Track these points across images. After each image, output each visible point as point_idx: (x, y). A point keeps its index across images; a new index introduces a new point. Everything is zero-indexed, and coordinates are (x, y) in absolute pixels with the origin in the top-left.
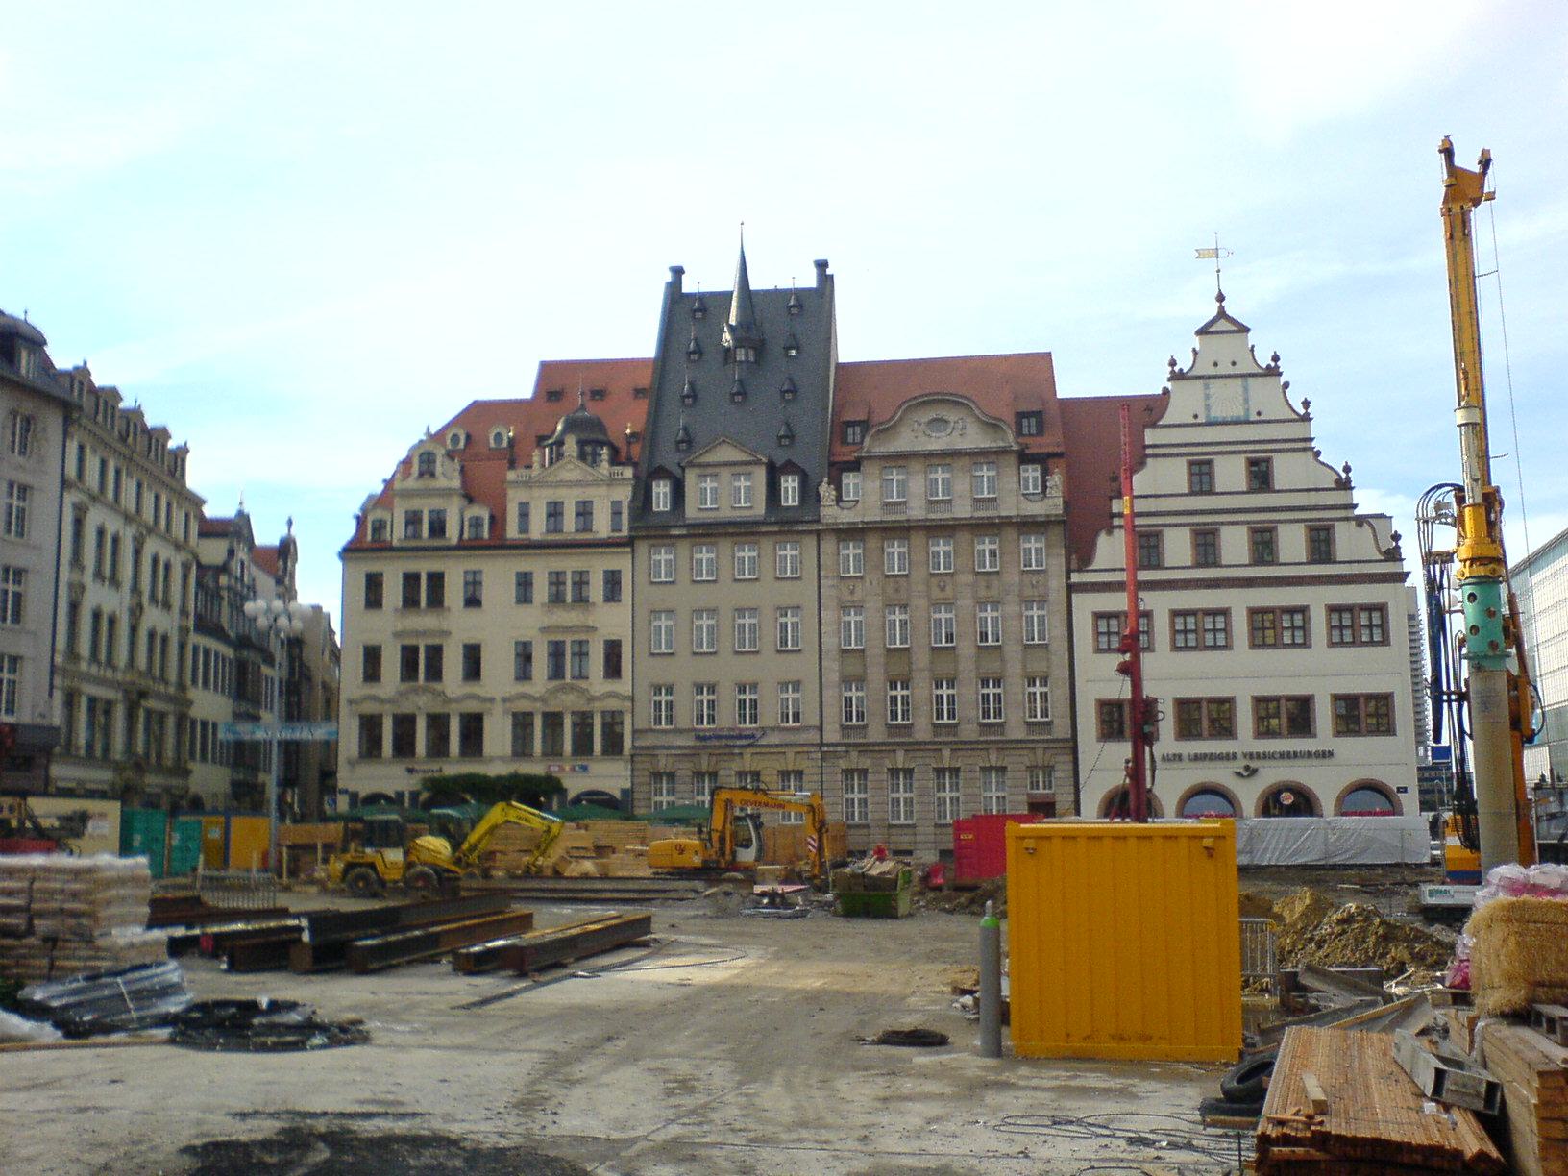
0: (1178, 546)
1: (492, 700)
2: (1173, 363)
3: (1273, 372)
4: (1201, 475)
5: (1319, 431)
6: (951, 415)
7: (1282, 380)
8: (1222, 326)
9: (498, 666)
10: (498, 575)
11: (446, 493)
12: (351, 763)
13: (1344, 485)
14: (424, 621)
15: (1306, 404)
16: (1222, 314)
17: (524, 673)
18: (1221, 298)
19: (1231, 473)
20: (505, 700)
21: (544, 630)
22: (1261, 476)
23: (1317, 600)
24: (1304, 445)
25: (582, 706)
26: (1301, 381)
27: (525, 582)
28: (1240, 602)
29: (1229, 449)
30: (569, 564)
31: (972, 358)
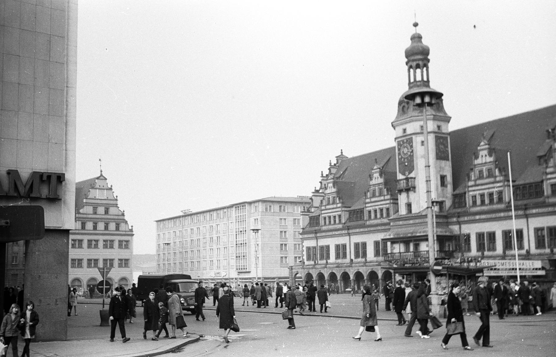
0: (89, 226)
3: (111, 189)
4: (95, 209)
5: (119, 203)
8: (101, 177)
13: (123, 215)
15: (117, 197)
16: (101, 175)
18: (101, 171)
19: (101, 210)
22: (107, 212)
23: (117, 238)
24: (116, 206)
26: (116, 192)
28: (101, 238)
29: (102, 205)
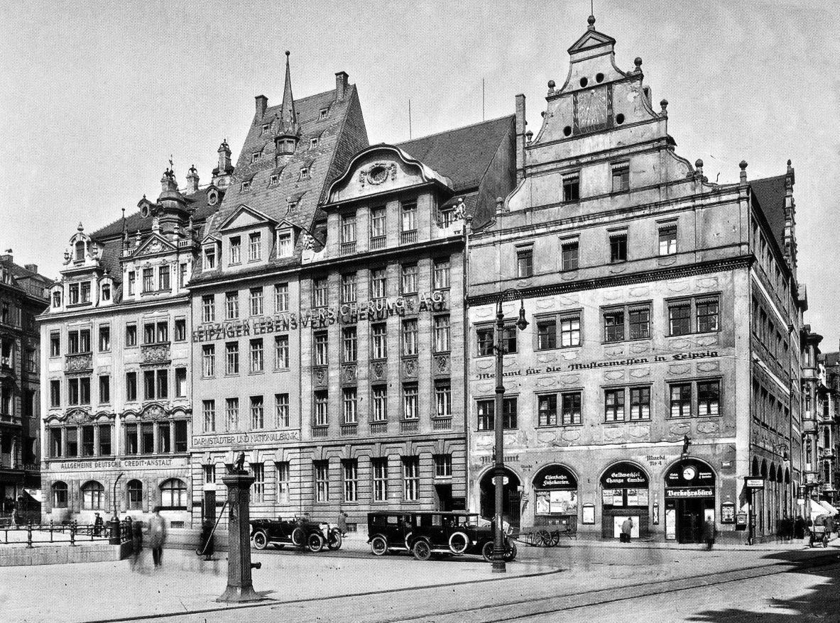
1: (114, 416)
2: (552, 85)
6: (387, 163)
7: (645, 83)
9: (118, 388)
10: (118, 325)
11: (89, 272)
12: (47, 462)
14: (79, 364)
17: (132, 395)
18: (591, 21)
20: (121, 416)
21: (142, 365)
25: (163, 418)
27: (131, 330)
30: (155, 317)
31: (361, 116)
